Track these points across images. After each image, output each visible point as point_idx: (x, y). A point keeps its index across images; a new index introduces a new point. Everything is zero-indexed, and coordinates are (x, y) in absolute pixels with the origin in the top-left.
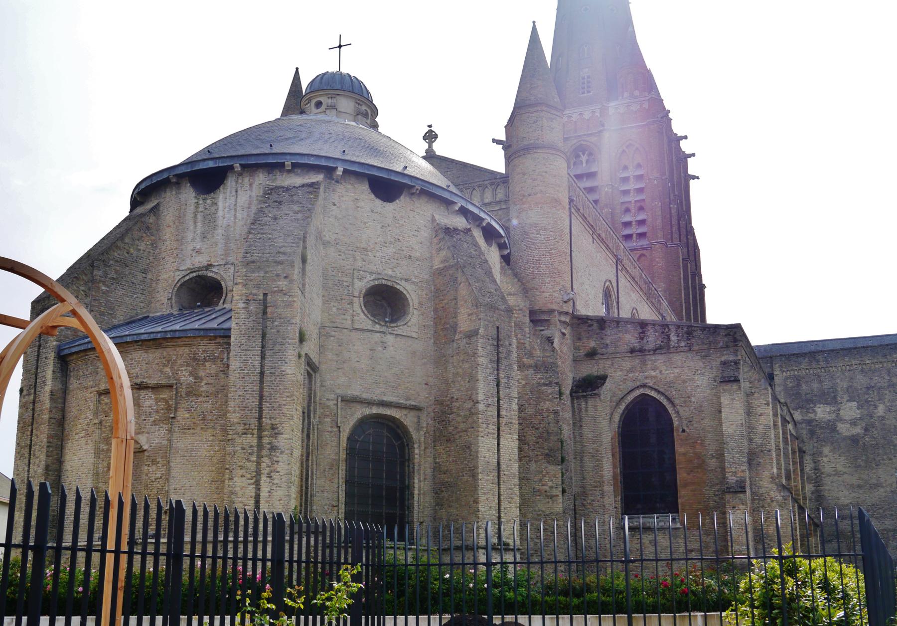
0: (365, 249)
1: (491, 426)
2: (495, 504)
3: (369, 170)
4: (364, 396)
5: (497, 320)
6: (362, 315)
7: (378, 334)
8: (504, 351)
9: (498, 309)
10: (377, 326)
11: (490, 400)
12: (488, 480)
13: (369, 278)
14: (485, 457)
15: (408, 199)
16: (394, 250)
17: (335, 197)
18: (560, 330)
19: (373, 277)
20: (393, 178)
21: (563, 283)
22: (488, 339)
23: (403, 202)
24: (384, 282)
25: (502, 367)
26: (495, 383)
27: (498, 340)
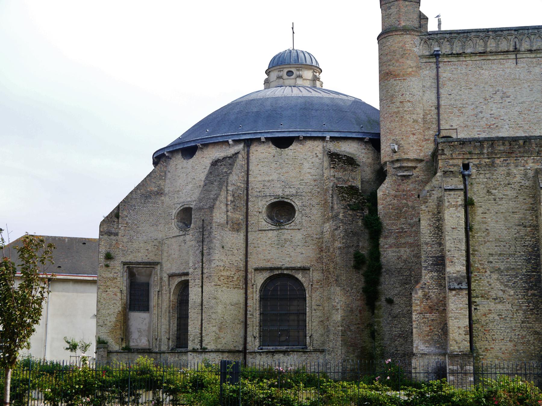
0: (178, 191)
1: (197, 281)
2: (199, 326)
3: (175, 147)
4: (177, 272)
5: (203, 215)
6: (175, 229)
7: (182, 237)
8: (207, 233)
9: (203, 209)
10: (181, 232)
11: (196, 265)
12: (194, 312)
13: (179, 206)
14: (193, 299)
15: (200, 152)
16: (192, 186)
17: (169, 168)
18: (397, 175)
19: (180, 205)
20: (186, 146)
21: (394, 138)
22: (197, 229)
23: (198, 154)
24: (185, 206)
25: (205, 243)
26: (200, 255)
27: (203, 227)
